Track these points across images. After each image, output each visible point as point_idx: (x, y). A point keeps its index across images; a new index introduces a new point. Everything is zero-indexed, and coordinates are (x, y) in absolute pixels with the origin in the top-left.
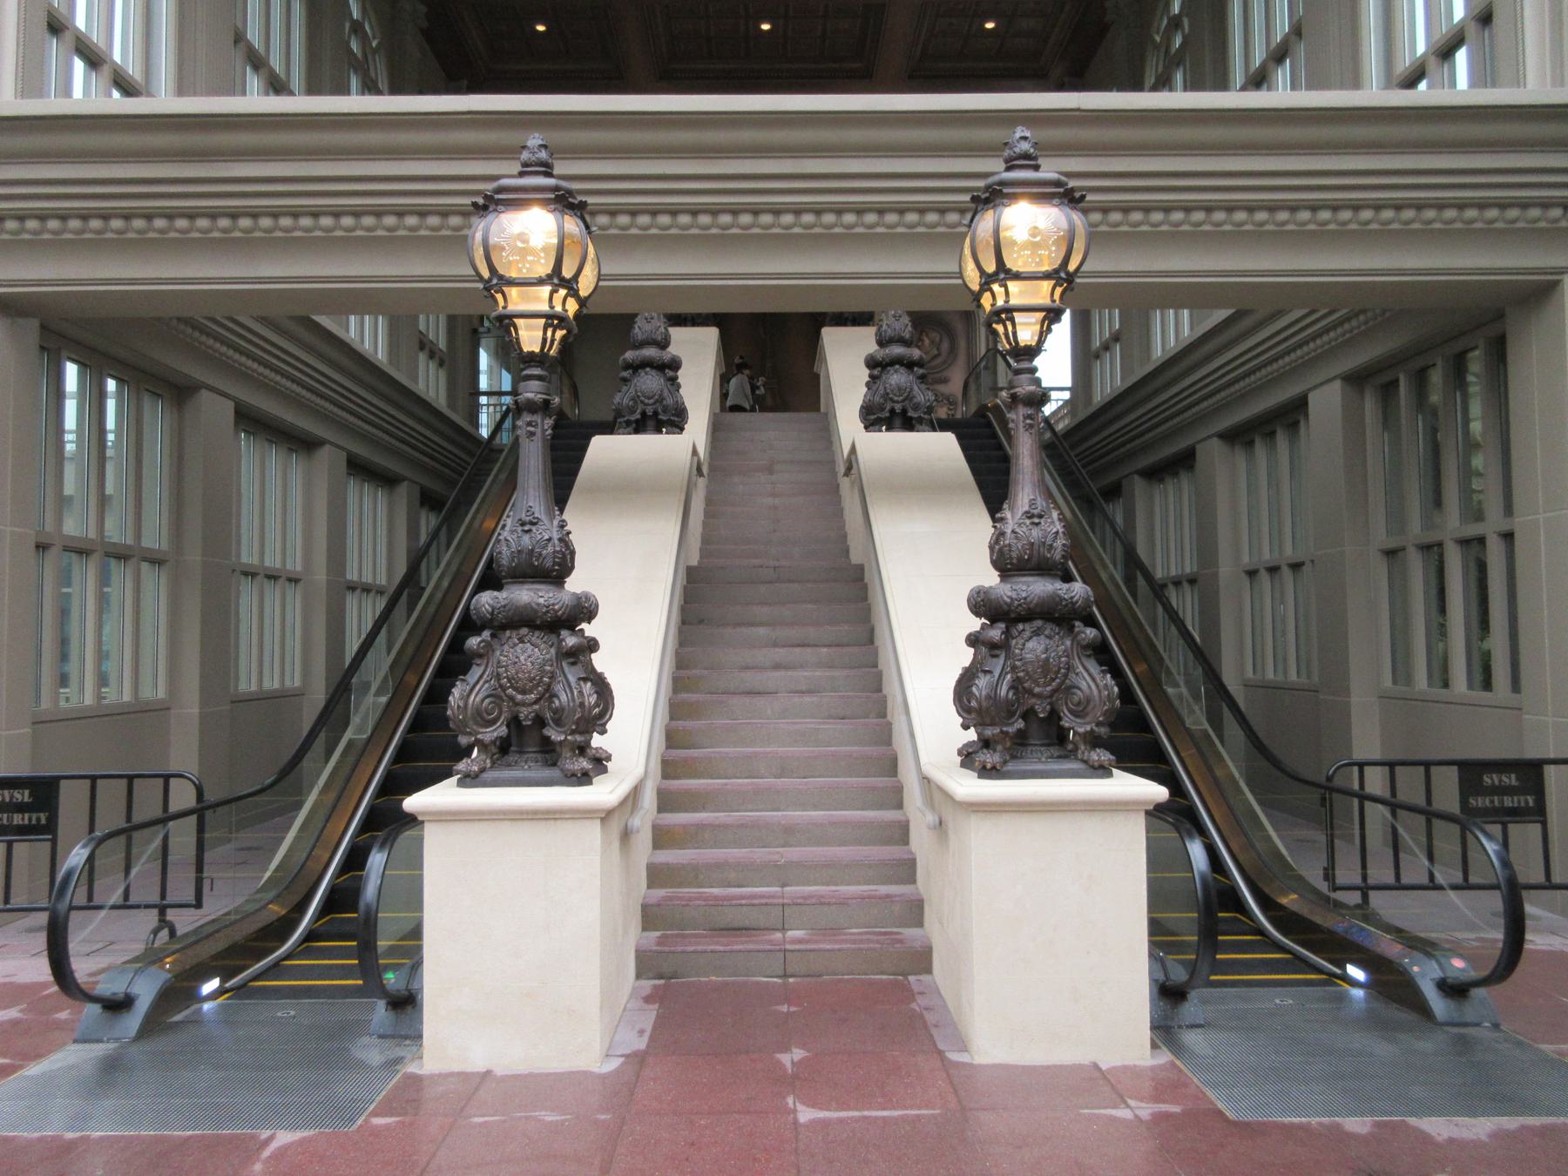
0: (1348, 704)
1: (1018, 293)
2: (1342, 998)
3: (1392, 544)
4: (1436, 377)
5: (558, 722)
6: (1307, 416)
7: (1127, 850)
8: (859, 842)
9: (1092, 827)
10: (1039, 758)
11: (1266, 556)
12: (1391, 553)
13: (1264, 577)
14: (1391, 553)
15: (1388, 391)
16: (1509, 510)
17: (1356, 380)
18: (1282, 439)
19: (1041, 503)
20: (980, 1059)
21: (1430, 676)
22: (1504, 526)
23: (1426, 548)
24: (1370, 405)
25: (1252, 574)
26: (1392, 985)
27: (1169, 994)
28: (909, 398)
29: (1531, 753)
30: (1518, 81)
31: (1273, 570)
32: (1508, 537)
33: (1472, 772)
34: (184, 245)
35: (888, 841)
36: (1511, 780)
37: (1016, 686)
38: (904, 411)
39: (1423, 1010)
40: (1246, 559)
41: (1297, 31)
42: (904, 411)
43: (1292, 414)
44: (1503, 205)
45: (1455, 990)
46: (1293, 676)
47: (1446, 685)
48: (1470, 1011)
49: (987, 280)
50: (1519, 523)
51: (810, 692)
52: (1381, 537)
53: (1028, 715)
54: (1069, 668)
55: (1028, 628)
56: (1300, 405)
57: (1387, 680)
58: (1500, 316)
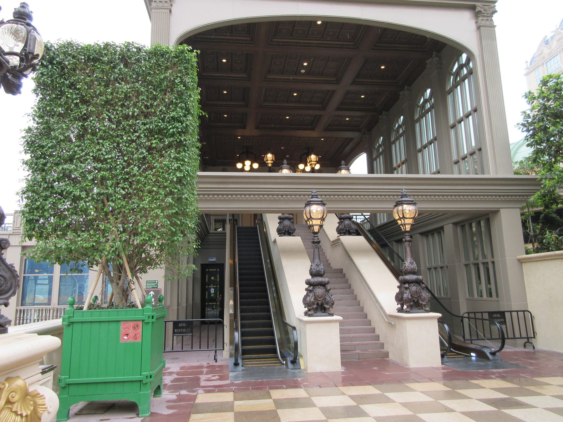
0: (459, 302)
1: (407, 221)
2: (471, 360)
3: (467, 263)
4: (474, 225)
5: (327, 304)
6: (443, 231)
7: (434, 327)
8: (364, 333)
9: (428, 322)
10: (415, 309)
11: (433, 265)
12: (466, 265)
13: (433, 270)
14: (466, 265)
15: (463, 227)
16: (493, 257)
17: (455, 224)
18: (436, 236)
19: (412, 261)
20: (411, 367)
21: (478, 295)
22: (492, 260)
23: (474, 264)
24: (459, 230)
25: (429, 269)
26: (481, 355)
27: (442, 356)
28: (350, 227)
29: (502, 310)
30: (489, 173)
31: (435, 268)
32: (493, 263)
33: (491, 314)
34: (215, 201)
35: (370, 332)
36: (499, 316)
37: (411, 295)
38: (349, 230)
39: (487, 358)
40: (428, 265)
41: (435, 139)
42: (349, 230)
43: (440, 230)
44: (488, 196)
45: (493, 354)
46: (443, 295)
47: (482, 296)
48: (496, 358)
49: (400, 219)
50: (495, 260)
51: (340, 300)
52: (464, 261)
53: (414, 301)
54: (421, 292)
55: (412, 285)
56: (442, 228)
57: (468, 296)
58: (488, 214)
